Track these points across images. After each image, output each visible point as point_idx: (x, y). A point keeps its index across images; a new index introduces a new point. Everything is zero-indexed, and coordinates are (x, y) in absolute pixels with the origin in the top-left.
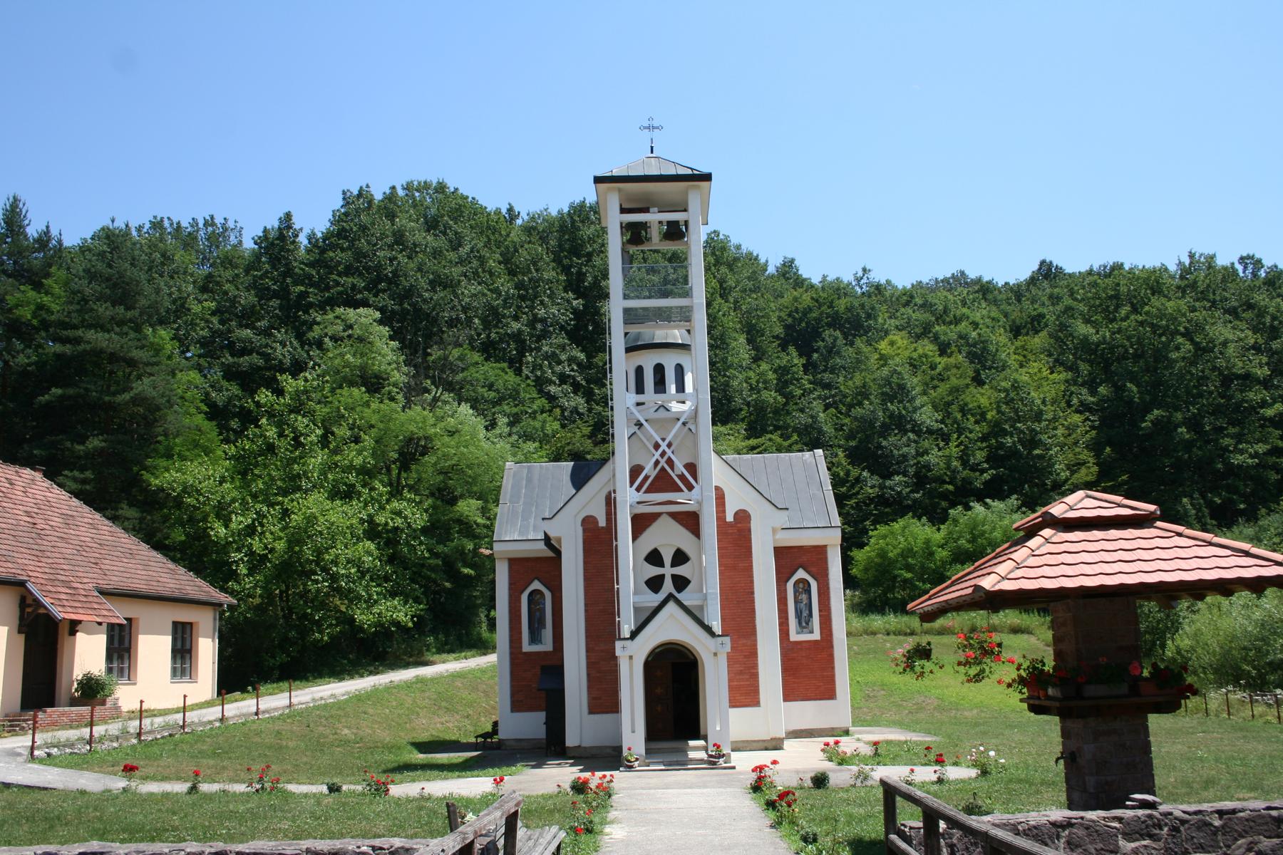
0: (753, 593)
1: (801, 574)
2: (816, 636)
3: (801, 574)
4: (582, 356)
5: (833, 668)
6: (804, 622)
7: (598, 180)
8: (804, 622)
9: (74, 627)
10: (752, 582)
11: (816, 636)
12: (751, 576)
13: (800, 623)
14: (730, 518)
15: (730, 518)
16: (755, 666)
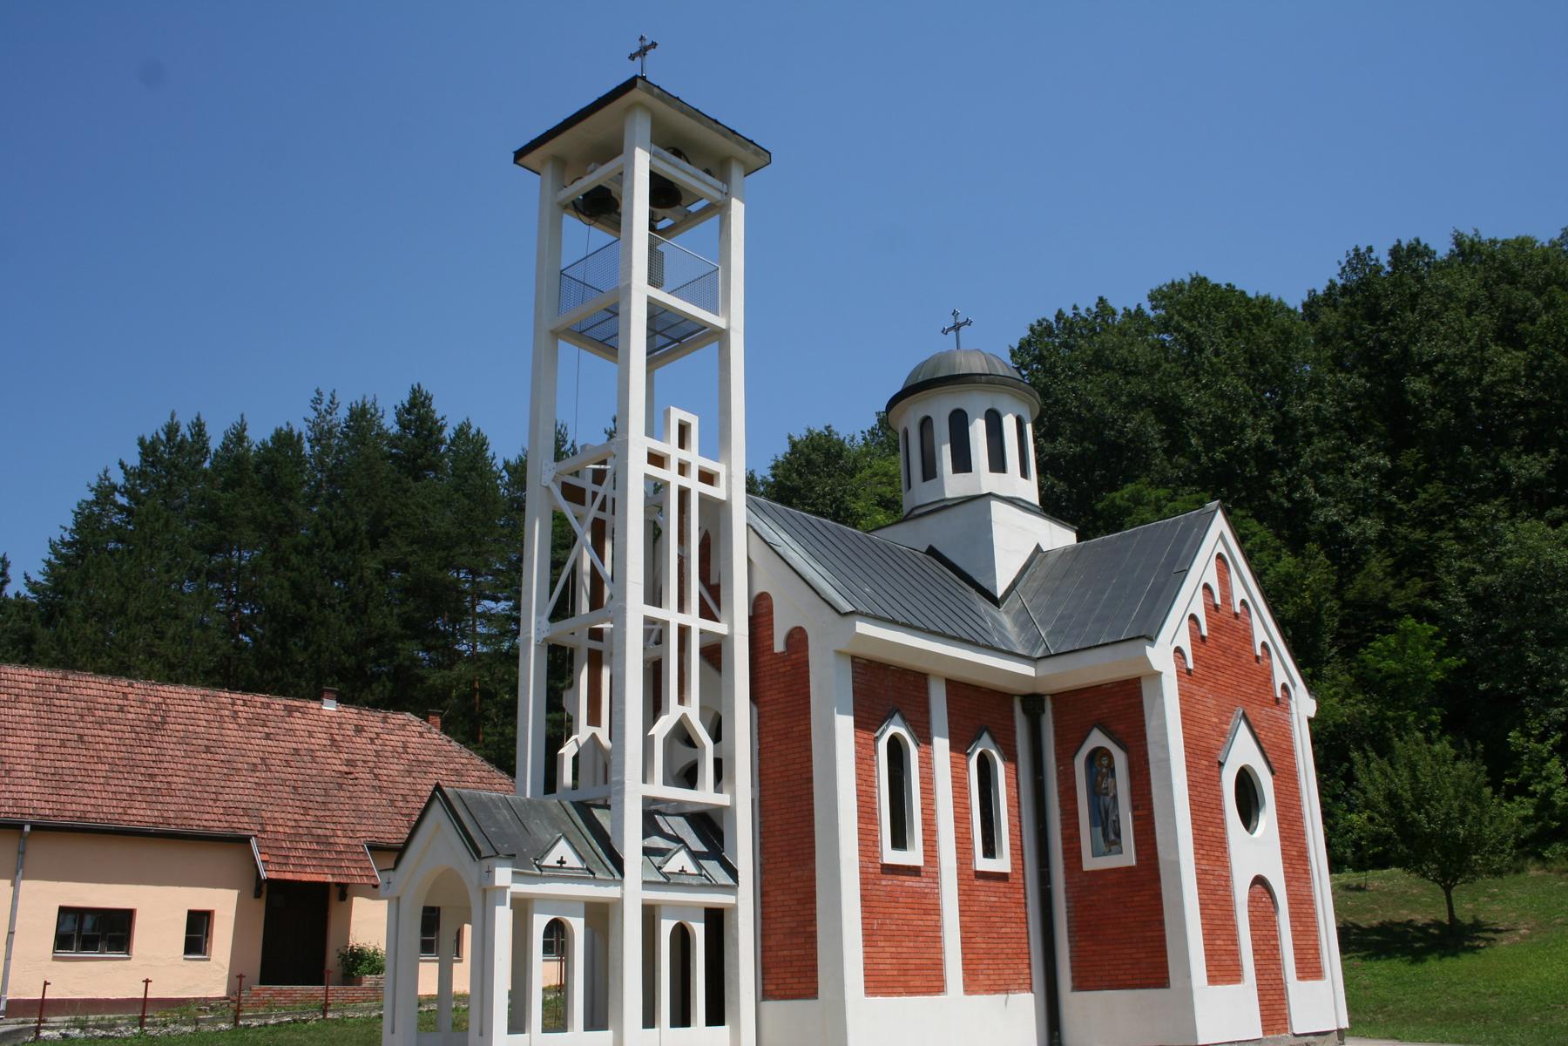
0: (810, 780)
1: (1097, 739)
2: (1127, 857)
3: (1097, 739)
4: (1384, 462)
5: (1162, 922)
6: (1109, 838)
7: (519, 155)
8: (1109, 838)
9: (344, 892)
10: (809, 759)
11: (1127, 857)
12: (809, 749)
13: (1105, 835)
14: (779, 646)
15: (779, 646)
16: (812, 920)
